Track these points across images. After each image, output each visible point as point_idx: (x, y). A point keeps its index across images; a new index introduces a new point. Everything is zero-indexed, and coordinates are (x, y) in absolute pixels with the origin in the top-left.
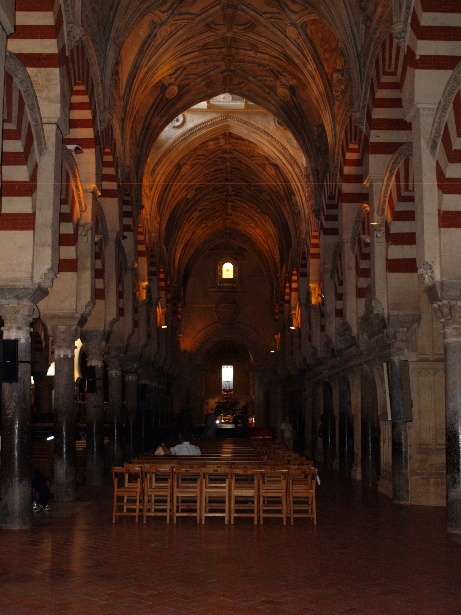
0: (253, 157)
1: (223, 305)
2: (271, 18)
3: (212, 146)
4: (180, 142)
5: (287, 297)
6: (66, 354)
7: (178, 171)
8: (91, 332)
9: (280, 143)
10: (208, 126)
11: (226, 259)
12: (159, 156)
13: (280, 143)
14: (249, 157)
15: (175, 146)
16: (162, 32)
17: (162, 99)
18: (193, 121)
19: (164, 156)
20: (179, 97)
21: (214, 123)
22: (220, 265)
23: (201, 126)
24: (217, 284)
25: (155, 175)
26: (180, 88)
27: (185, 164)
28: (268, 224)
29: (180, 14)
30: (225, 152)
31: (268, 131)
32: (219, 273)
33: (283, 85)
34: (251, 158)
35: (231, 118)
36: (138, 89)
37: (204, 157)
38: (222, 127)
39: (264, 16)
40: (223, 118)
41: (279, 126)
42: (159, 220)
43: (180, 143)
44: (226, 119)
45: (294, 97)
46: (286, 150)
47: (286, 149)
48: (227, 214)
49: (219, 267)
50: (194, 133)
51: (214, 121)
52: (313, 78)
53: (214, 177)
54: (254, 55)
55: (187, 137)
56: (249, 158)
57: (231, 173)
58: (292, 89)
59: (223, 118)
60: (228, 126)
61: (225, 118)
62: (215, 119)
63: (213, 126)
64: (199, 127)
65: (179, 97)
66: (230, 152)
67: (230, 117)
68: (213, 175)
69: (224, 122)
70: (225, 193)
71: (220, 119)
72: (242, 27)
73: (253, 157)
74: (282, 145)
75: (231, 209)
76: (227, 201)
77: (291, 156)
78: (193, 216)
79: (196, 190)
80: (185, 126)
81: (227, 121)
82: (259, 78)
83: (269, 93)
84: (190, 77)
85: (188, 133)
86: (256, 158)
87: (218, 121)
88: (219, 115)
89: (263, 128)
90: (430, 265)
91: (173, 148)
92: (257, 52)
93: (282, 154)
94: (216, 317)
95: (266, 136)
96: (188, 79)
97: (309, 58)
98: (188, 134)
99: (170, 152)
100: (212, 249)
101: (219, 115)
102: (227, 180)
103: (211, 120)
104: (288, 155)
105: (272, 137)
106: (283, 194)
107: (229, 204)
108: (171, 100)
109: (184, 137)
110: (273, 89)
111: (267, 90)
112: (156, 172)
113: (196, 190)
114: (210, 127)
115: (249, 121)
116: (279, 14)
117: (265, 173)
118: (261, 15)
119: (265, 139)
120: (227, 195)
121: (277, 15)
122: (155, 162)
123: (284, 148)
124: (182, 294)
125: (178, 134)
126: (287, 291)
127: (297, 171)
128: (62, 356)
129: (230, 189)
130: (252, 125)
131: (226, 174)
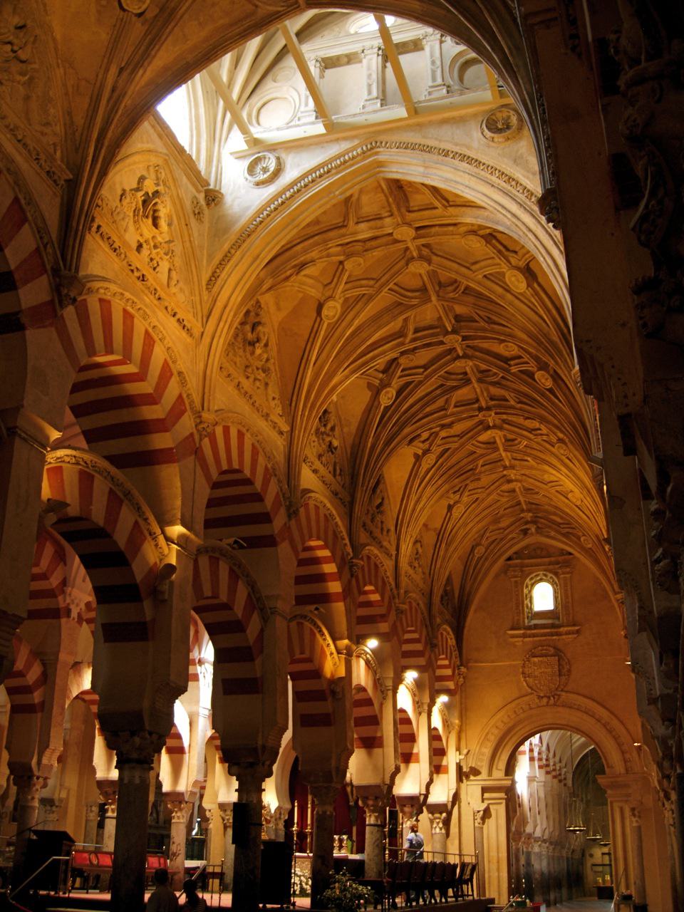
1: (536, 659)
4: (271, 212)
7: (318, 319)
9: (500, 171)
10: (333, 171)
11: (537, 576)
12: (226, 247)
13: (500, 171)
14: (468, 265)
15: (261, 222)
18: (299, 165)
19: (237, 245)
21: (345, 162)
22: (527, 587)
23: (318, 173)
24: (524, 621)
25: (216, 289)
28: (577, 464)
31: (468, 153)
32: (527, 602)
34: (474, 268)
35: (383, 144)
37: (372, 282)
38: (366, 168)
40: (364, 148)
41: (493, 135)
42: (286, 428)
43: (272, 215)
44: (372, 149)
46: (513, 183)
47: (514, 180)
49: (526, 591)
50: (303, 190)
51: (347, 158)
55: (287, 199)
56: (468, 268)
59: (364, 148)
60: (380, 164)
61: (369, 146)
62: (347, 152)
63: (347, 168)
64: (314, 175)
67: (381, 143)
69: (369, 157)
70: (476, 406)
71: (359, 150)
74: (503, 173)
75: (505, 450)
77: (528, 191)
80: (280, 179)
81: (377, 153)
85: (289, 190)
86: (482, 264)
87: (354, 158)
88: (356, 142)
89: (456, 149)
91: (257, 226)
93: (506, 194)
94: (525, 684)
95: (465, 165)
98: (288, 194)
99: (249, 235)
100: (509, 559)
101: (356, 142)
103: (338, 157)
104: (521, 191)
105: (478, 163)
106: (555, 337)
109: (280, 200)
112: (219, 282)
114: (338, 173)
115: (423, 141)
117: (509, 296)
119: (464, 172)
122: (216, 261)
123: (510, 179)
125: (265, 196)
130: (428, 149)
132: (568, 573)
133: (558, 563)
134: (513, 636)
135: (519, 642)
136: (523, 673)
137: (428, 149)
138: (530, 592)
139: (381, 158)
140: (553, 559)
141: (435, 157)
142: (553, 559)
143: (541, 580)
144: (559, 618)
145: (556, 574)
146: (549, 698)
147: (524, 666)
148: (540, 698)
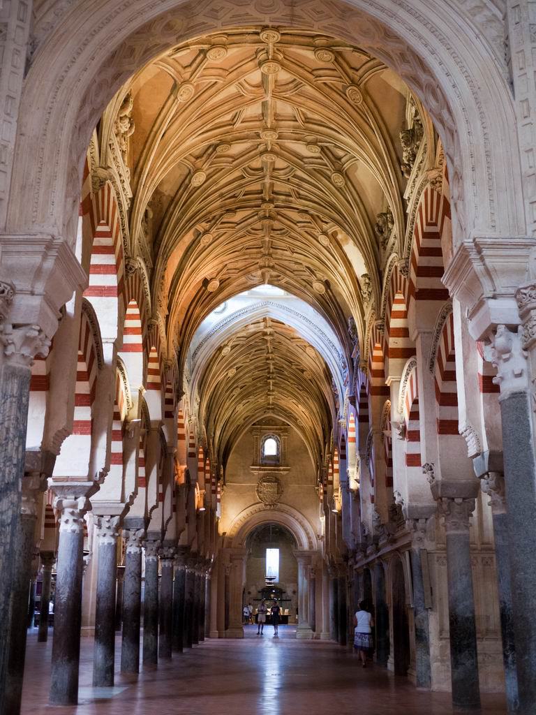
0: (293, 338)
1: (265, 484)
2: (304, 227)
3: (252, 329)
5: (330, 478)
6: (110, 542)
8: (131, 519)
16: (206, 240)
17: (204, 291)
20: (221, 290)
26: (222, 282)
27: (226, 345)
29: (222, 223)
30: (265, 334)
31: (307, 317)
33: (319, 280)
36: (181, 289)
39: (298, 224)
45: (329, 290)
48: (269, 390)
49: (261, 443)
52: (344, 280)
53: (255, 357)
54: (290, 255)
57: (272, 353)
58: (327, 284)
65: (221, 290)
66: (271, 334)
68: (254, 355)
72: (279, 232)
73: (293, 338)
76: (269, 378)
78: (234, 393)
79: (237, 369)
82: (296, 273)
83: (305, 287)
84: (229, 271)
88: (259, 300)
90: (431, 466)
92: (293, 253)
95: (304, 321)
96: (229, 273)
97: (340, 261)
102: (268, 359)
106: (323, 376)
107: (271, 381)
108: (212, 293)
110: (310, 283)
111: (304, 283)
113: (237, 369)
116: (310, 222)
118: (295, 224)
120: (269, 373)
121: (309, 224)
124: (222, 473)
126: (330, 471)
127: (335, 355)
128: (106, 544)
129: (272, 367)
131: (268, 353)
132: (286, 436)
133: (281, 429)
134: (253, 469)
135: (256, 473)
136: (257, 490)
137: (290, 311)
138: (264, 444)
139: (268, 309)
140: (278, 427)
141: (293, 315)
142: (278, 427)
143: (270, 438)
144: (279, 461)
145: (279, 435)
146: (270, 505)
147: (258, 487)
148: (265, 505)
